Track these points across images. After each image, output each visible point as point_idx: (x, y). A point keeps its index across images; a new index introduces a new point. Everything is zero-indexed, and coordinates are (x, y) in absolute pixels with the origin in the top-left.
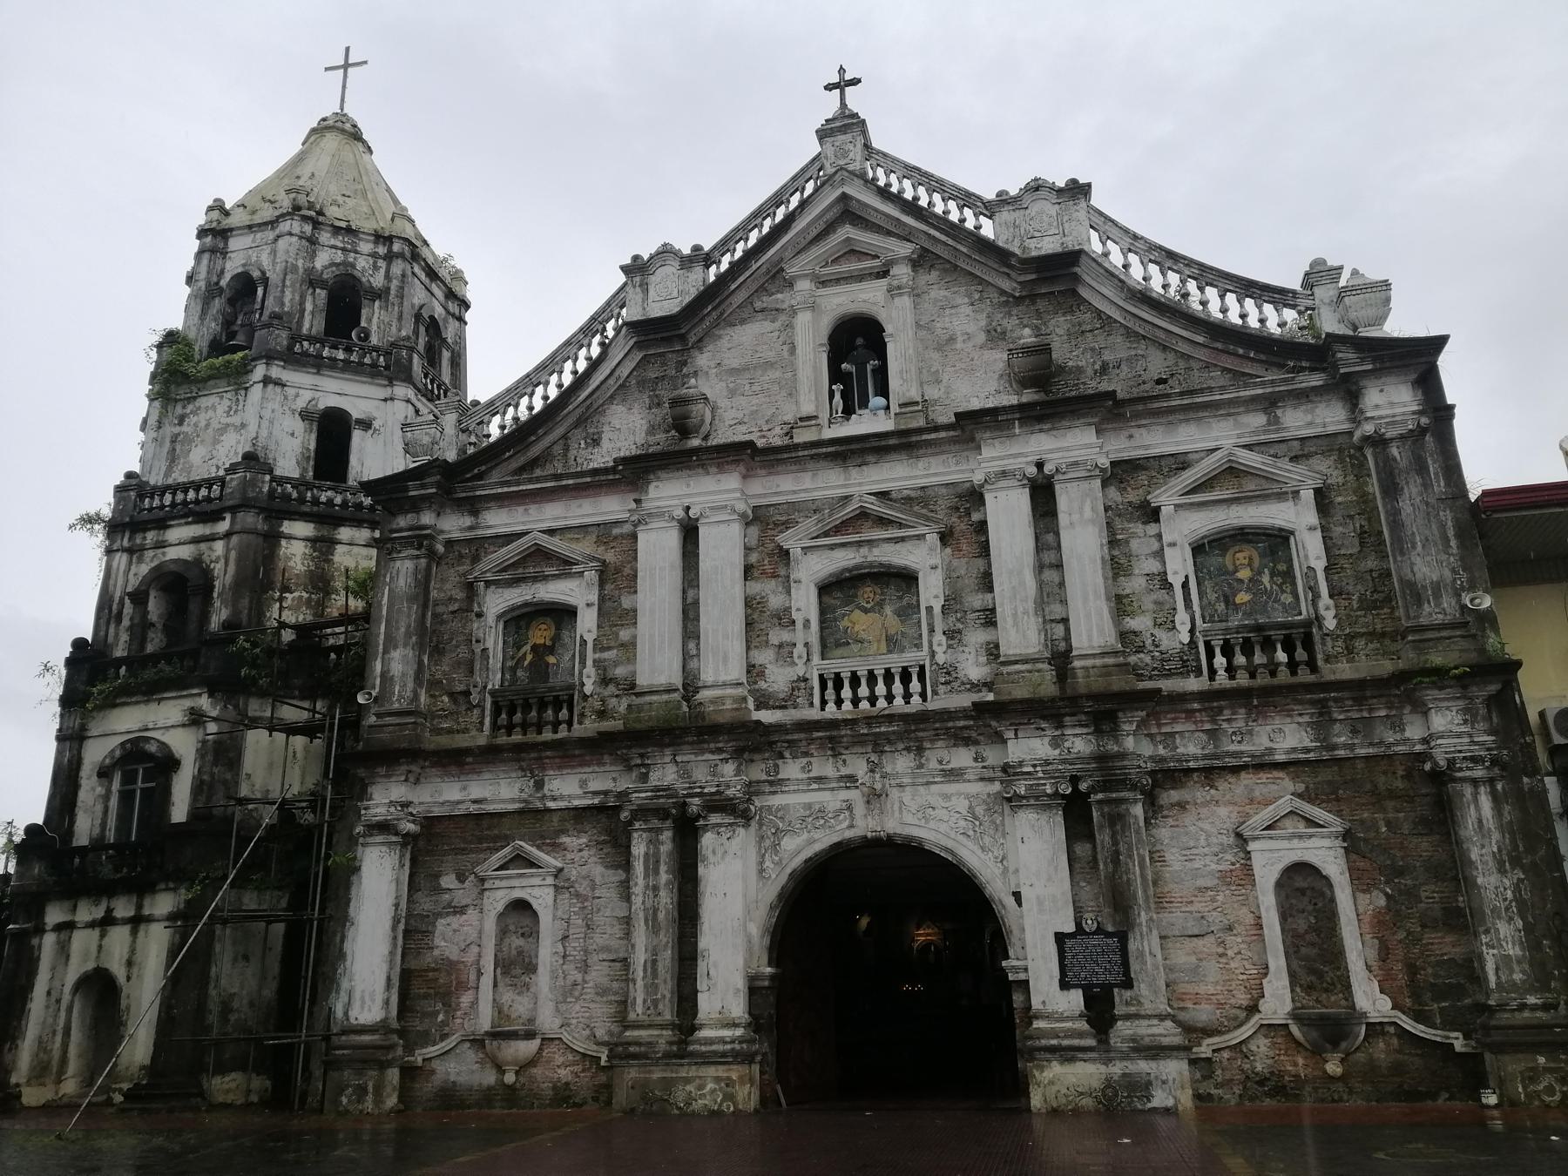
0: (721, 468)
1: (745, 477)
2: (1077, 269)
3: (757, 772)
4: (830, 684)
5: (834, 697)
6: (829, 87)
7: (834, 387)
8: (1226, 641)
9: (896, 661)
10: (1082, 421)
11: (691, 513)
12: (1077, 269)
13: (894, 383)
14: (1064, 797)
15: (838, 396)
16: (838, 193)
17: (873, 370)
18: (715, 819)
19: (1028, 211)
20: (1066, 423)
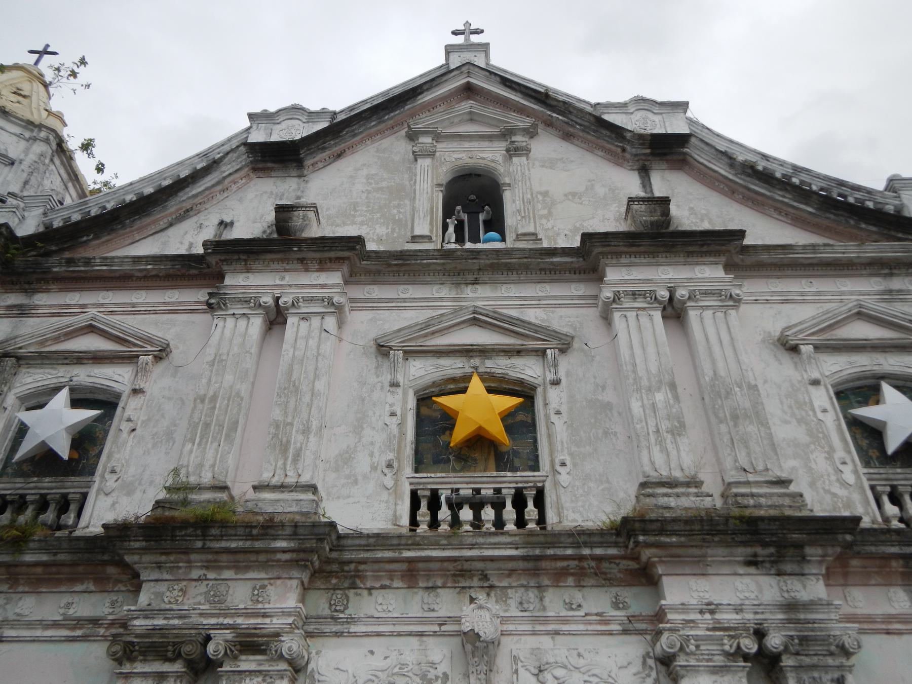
0: (323, 266)
1: (346, 282)
2: (688, 150)
3: (320, 603)
4: (424, 504)
5: (428, 518)
6: (455, 33)
7: (448, 220)
8: (893, 488)
9: (509, 482)
10: (712, 259)
11: (281, 302)
12: (686, 150)
13: (511, 219)
14: (746, 657)
15: (451, 229)
16: (462, 81)
17: (485, 222)
18: (248, 663)
19: (632, 116)
20: (695, 259)
